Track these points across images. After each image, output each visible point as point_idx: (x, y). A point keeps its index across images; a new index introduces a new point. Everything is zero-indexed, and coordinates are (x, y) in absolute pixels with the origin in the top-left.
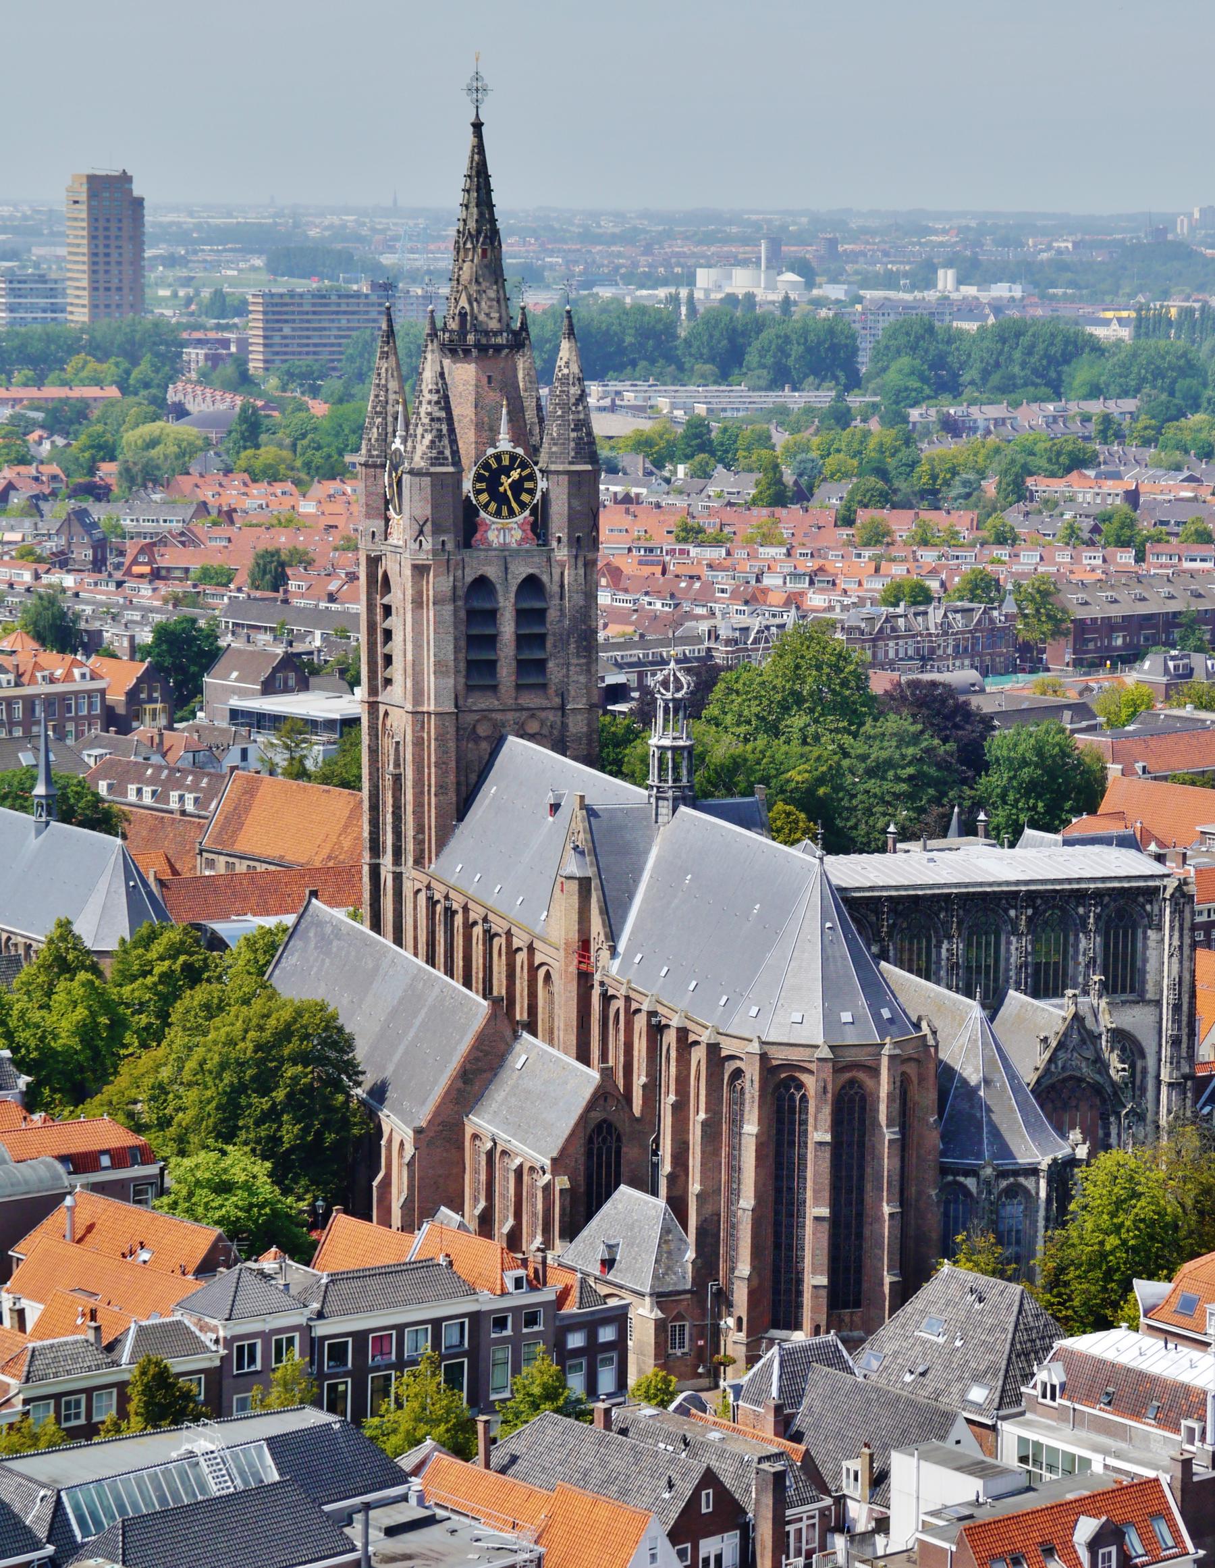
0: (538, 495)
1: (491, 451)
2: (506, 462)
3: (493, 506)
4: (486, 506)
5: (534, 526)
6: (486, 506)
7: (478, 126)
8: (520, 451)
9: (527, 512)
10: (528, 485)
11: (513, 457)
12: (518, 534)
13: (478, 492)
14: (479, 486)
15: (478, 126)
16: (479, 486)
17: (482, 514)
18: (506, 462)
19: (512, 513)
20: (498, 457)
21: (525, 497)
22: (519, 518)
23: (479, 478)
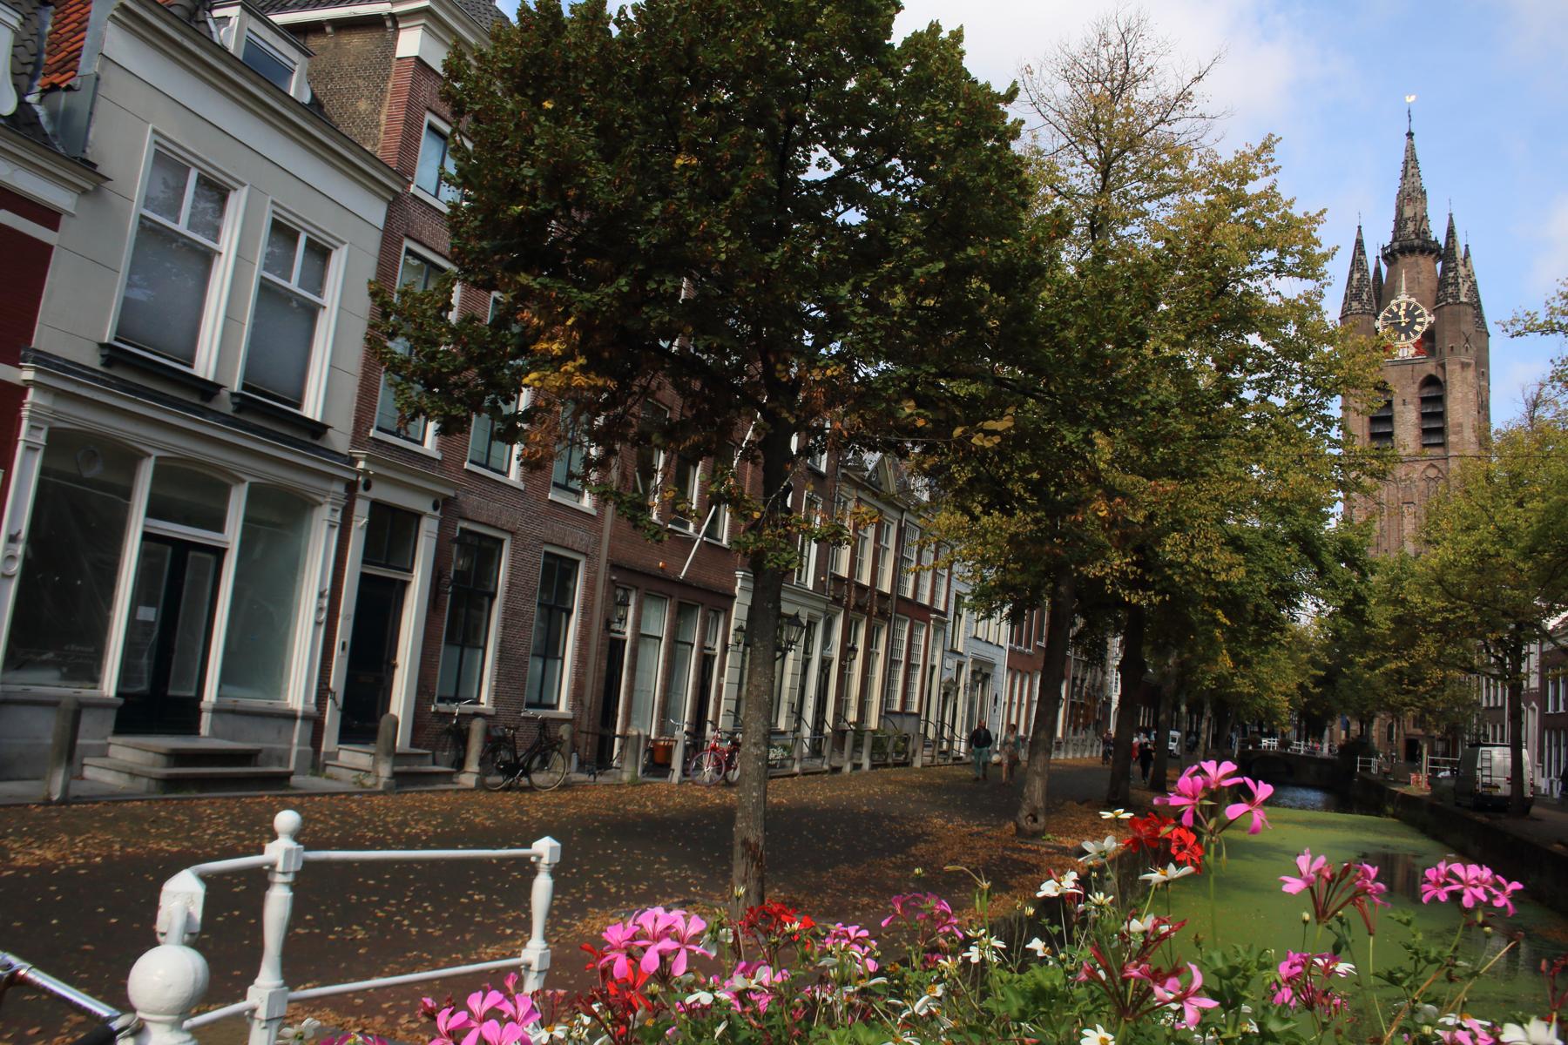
7: (1410, 135)
10: (1418, 320)
13: (1385, 327)
15: (1410, 135)
21: (1417, 328)
23: (1386, 318)
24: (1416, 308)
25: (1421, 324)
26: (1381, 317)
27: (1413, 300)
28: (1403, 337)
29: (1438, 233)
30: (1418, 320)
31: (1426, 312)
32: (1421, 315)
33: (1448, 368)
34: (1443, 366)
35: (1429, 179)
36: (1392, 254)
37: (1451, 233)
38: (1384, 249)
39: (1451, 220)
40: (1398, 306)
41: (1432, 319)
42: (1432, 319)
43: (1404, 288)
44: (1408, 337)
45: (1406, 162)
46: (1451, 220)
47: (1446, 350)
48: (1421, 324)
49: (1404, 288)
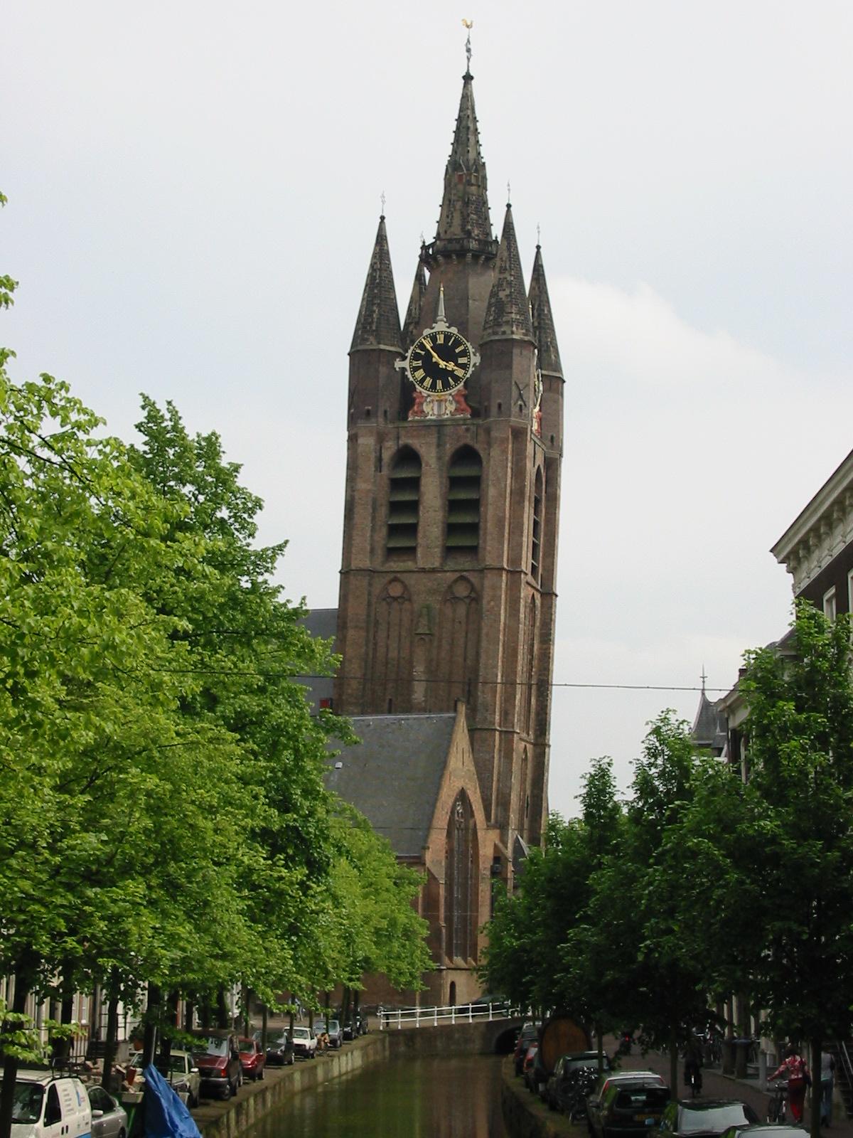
0: (471, 369)
1: (427, 332)
2: (441, 340)
3: (428, 381)
4: (423, 380)
6: (423, 380)
7: (468, 78)
8: (454, 330)
11: (447, 336)
13: (415, 369)
14: (415, 364)
15: (468, 78)
16: (415, 364)
18: (441, 340)
19: (446, 386)
22: (454, 391)
23: (416, 357)
24: (458, 343)
26: (409, 354)
27: (454, 330)
28: (439, 384)
29: (497, 231)
32: (465, 353)
33: (494, 434)
34: (488, 431)
35: (490, 149)
36: (434, 257)
38: (424, 247)
45: (459, 120)
47: (494, 410)
48: (464, 366)
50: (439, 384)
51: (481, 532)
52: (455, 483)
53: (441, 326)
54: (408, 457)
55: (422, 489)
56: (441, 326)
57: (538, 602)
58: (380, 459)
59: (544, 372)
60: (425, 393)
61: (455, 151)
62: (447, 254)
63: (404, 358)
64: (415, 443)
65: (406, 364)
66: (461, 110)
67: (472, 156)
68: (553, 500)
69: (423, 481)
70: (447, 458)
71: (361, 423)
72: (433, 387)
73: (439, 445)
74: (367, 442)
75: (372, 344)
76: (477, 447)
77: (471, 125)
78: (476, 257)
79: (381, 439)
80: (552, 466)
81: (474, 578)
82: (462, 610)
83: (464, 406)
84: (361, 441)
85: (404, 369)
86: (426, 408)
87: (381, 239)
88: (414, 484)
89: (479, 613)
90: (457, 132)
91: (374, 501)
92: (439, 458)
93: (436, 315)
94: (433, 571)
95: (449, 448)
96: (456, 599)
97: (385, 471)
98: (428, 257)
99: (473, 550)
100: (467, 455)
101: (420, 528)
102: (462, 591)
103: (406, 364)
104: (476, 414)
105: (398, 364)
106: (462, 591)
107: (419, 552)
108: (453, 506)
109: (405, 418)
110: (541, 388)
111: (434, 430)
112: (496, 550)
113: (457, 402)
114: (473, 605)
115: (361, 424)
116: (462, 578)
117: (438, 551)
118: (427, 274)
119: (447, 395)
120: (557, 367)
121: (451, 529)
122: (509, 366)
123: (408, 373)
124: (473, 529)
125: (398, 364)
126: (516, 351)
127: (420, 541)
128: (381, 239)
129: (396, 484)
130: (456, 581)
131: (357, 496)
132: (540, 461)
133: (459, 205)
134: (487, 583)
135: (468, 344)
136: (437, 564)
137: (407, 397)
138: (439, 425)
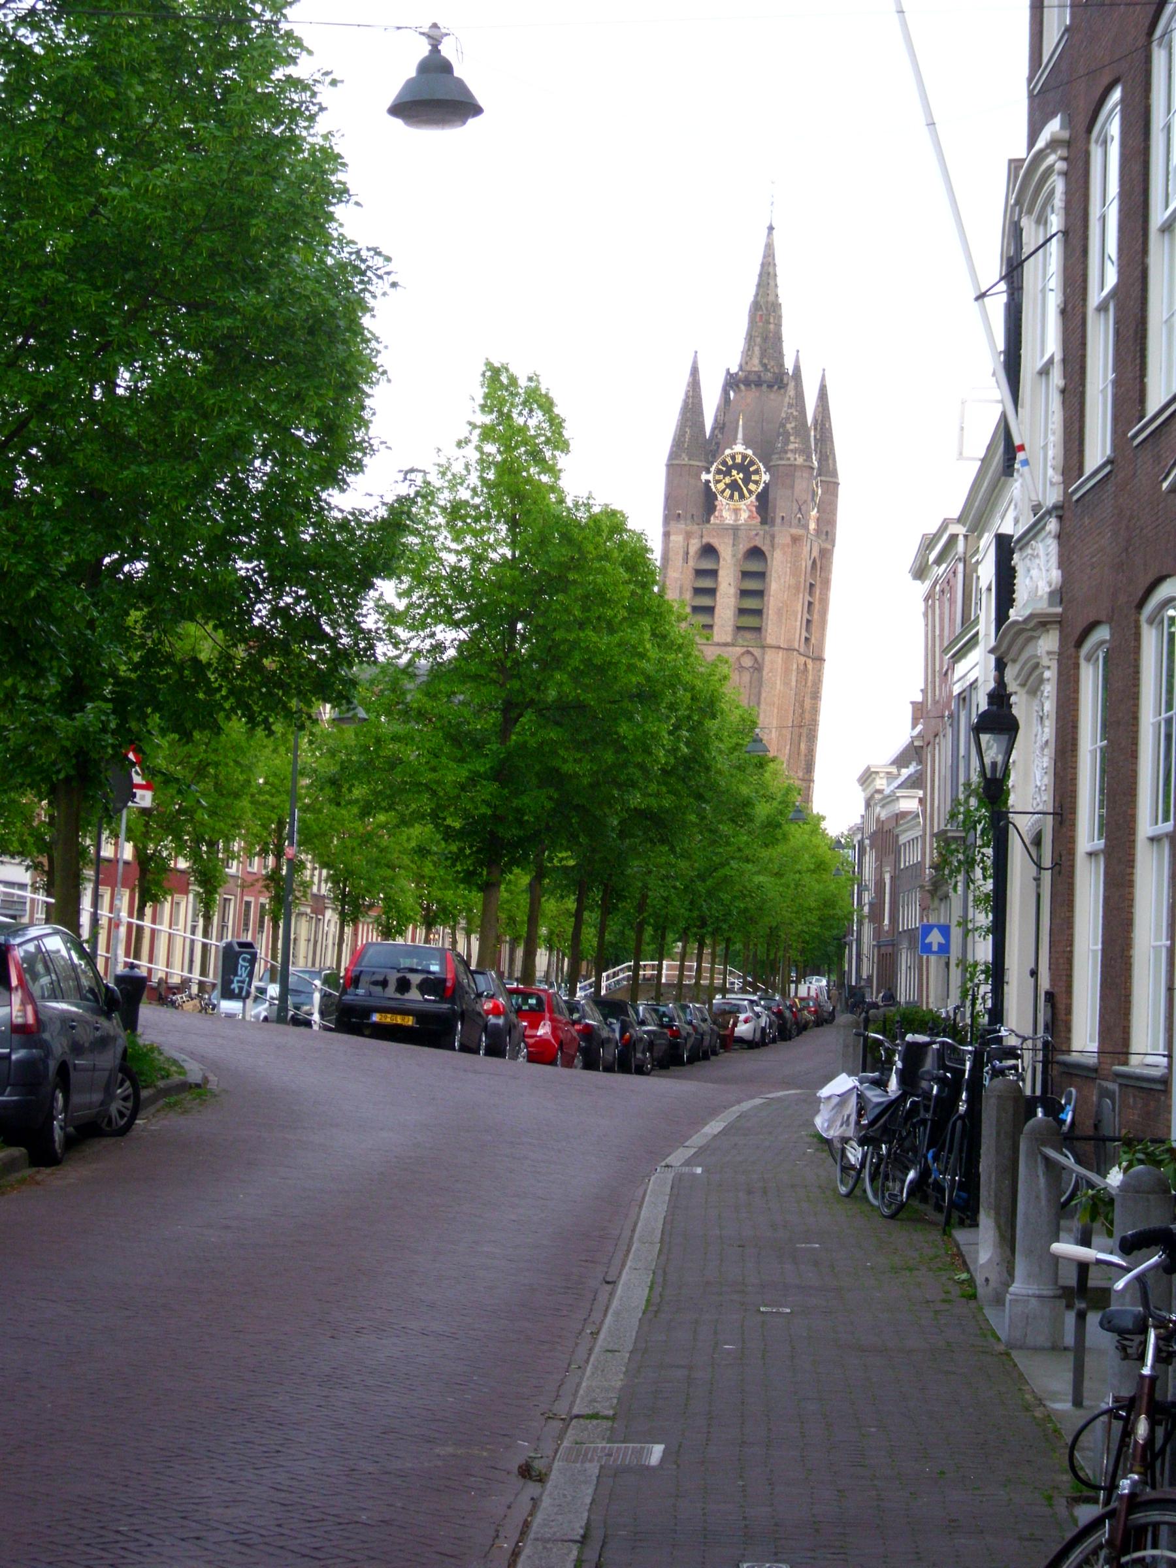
0: (762, 485)
1: (728, 452)
3: (728, 492)
4: (723, 492)
5: (757, 507)
6: (723, 492)
7: (771, 228)
8: (750, 452)
9: (754, 497)
10: (754, 477)
11: (745, 457)
12: (744, 515)
15: (771, 228)
17: (719, 497)
18: (739, 460)
19: (742, 497)
20: (733, 457)
21: (752, 486)
22: (748, 502)
23: (719, 472)
24: (752, 463)
25: (757, 483)
26: (713, 469)
27: (750, 452)
29: (789, 365)
30: (754, 477)
31: (763, 469)
32: (757, 472)
34: (773, 537)
37: (797, 369)
39: (797, 357)
40: (733, 457)
41: (766, 477)
42: (766, 477)
43: (740, 435)
44: (742, 497)
45: (763, 265)
46: (797, 357)
47: (778, 520)
48: (757, 483)
49: (740, 435)
50: (736, 494)
51: (764, 617)
52: (745, 575)
53: (739, 448)
54: (709, 551)
55: (720, 579)
56: (739, 448)
57: (810, 667)
58: (687, 553)
59: (823, 478)
60: (724, 501)
61: (757, 295)
62: (747, 383)
63: (708, 472)
64: (715, 542)
65: (710, 477)
66: (765, 257)
67: (771, 298)
68: (826, 583)
69: (721, 573)
70: (740, 556)
71: (673, 524)
72: (731, 497)
73: (734, 545)
74: (677, 539)
75: (685, 460)
76: (764, 548)
77: (771, 270)
78: (770, 386)
79: (688, 536)
80: (826, 555)
81: (757, 652)
82: (746, 677)
83: (755, 514)
84: (672, 538)
85: (708, 482)
86: (725, 514)
87: (695, 371)
88: (713, 573)
89: (760, 681)
90: (761, 276)
91: (681, 588)
92: (734, 556)
93: (735, 438)
94: (726, 645)
95: (743, 547)
96: (741, 668)
97: (691, 563)
98: (732, 382)
99: (758, 629)
100: (756, 553)
101: (717, 611)
102: (747, 662)
103: (710, 477)
104: (764, 521)
105: (704, 477)
106: (747, 662)
107: (716, 628)
108: (744, 593)
109: (708, 521)
110: (820, 491)
111: (731, 532)
112: (774, 631)
113: (751, 511)
114: (756, 674)
115: (674, 526)
116: (748, 652)
117: (729, 629)
118: (732, 394)
119: (742, 505)
120: (834, 473)
121: (742, 612)
122: (793, 487)
123: (712, 485)
124: (758, 613)
125: (704, 477)
126: (798, 474)
127: (716, 620)
128: (695, 371)
129: (700, 573)
130: (743, 654)
131: (671, 554)
132: (815, 553)
133: (758, 340)
134: (767, 658)
135: (761, 465)
136: (729, 639)
137: (709, 501)
138: (735, 529)
